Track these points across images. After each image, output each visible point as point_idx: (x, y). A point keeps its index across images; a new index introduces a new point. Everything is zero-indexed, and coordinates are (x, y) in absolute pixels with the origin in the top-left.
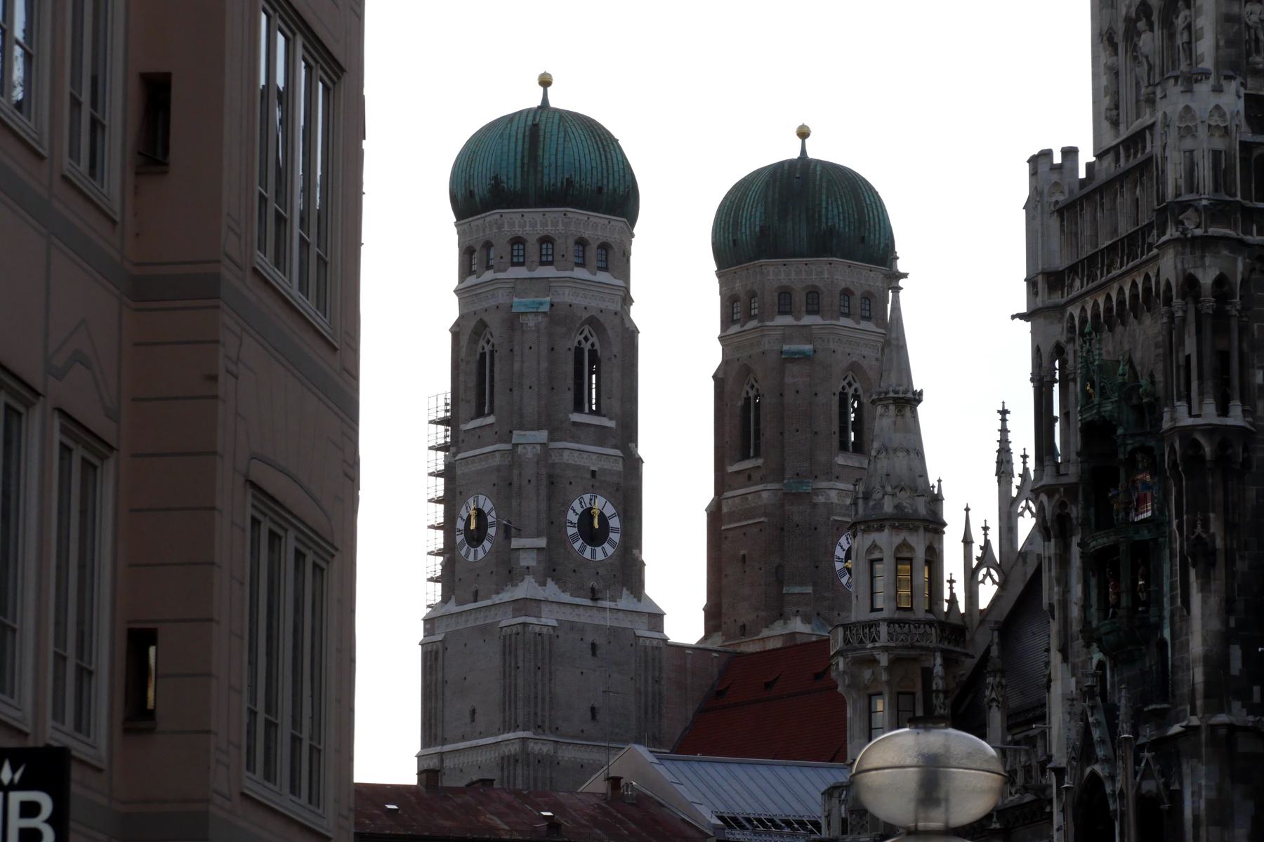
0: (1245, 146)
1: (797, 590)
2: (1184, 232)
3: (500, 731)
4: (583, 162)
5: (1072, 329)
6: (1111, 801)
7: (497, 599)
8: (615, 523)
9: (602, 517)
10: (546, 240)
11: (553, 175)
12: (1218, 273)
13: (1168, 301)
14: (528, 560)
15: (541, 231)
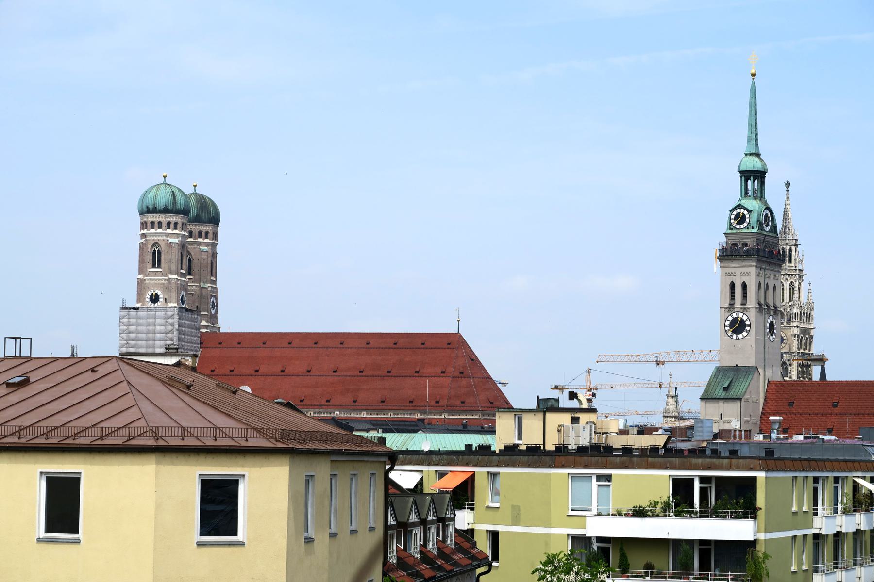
10: (176, 224)
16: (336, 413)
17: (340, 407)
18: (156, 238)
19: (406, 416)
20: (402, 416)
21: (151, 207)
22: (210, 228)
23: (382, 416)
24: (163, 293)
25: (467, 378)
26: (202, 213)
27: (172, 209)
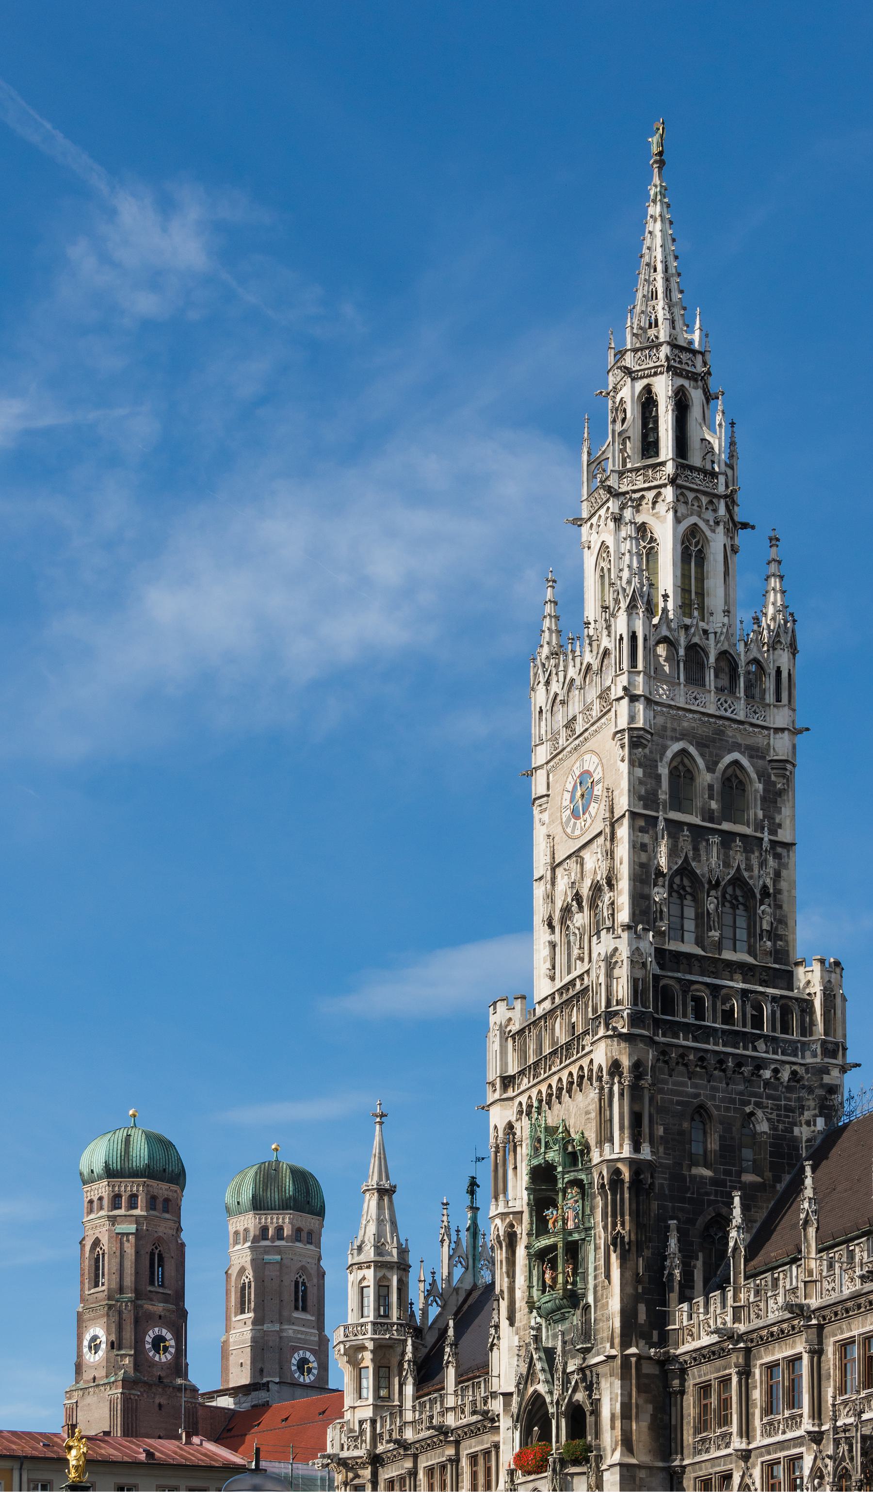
0: (656, 978)
2: (615, 1029)
4: (155, 1155)
5: (520, 1112)
6: (549, 1407)
11: (138, 1161)
12: (636, 1059)
13: (600, 1078)
24: (108, 1333)
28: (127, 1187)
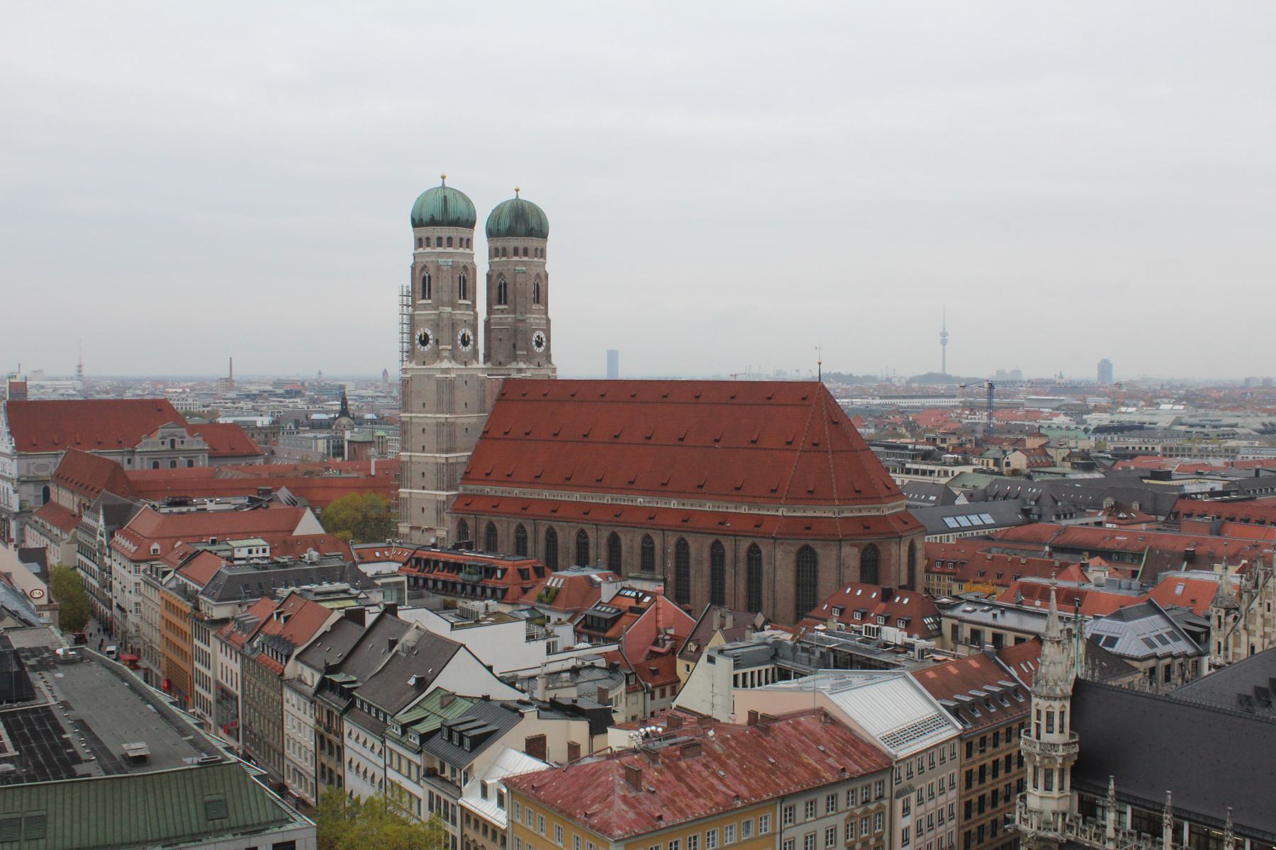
1: (522, 353)
3: (436, 413)
7: (433, 366)
8: (471, 338)
9: (468, 337)
10: (450, 240)
14: (445, 354)
15: (448, 235)
16: (639, 500)
17: (644, 492)
18: (423, 260)
19: (729, 510)
20: (725, 510)
21: (417, 219)
22: (532, 243)
23: (698, 508)
24: (433, 332)
25: (824, 451)
26: (517, 223)
27: (443, 220)
28: (445, 232)
